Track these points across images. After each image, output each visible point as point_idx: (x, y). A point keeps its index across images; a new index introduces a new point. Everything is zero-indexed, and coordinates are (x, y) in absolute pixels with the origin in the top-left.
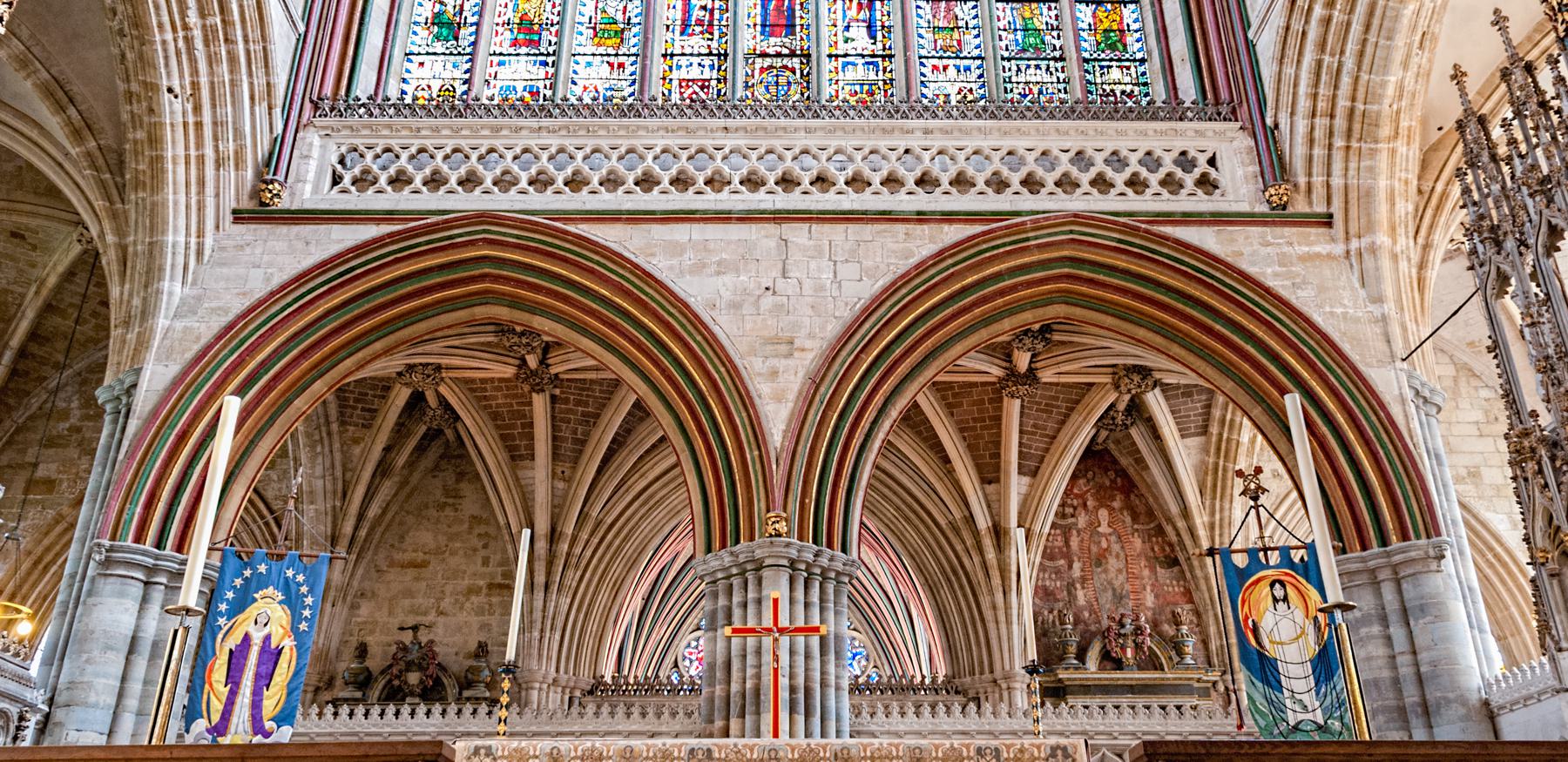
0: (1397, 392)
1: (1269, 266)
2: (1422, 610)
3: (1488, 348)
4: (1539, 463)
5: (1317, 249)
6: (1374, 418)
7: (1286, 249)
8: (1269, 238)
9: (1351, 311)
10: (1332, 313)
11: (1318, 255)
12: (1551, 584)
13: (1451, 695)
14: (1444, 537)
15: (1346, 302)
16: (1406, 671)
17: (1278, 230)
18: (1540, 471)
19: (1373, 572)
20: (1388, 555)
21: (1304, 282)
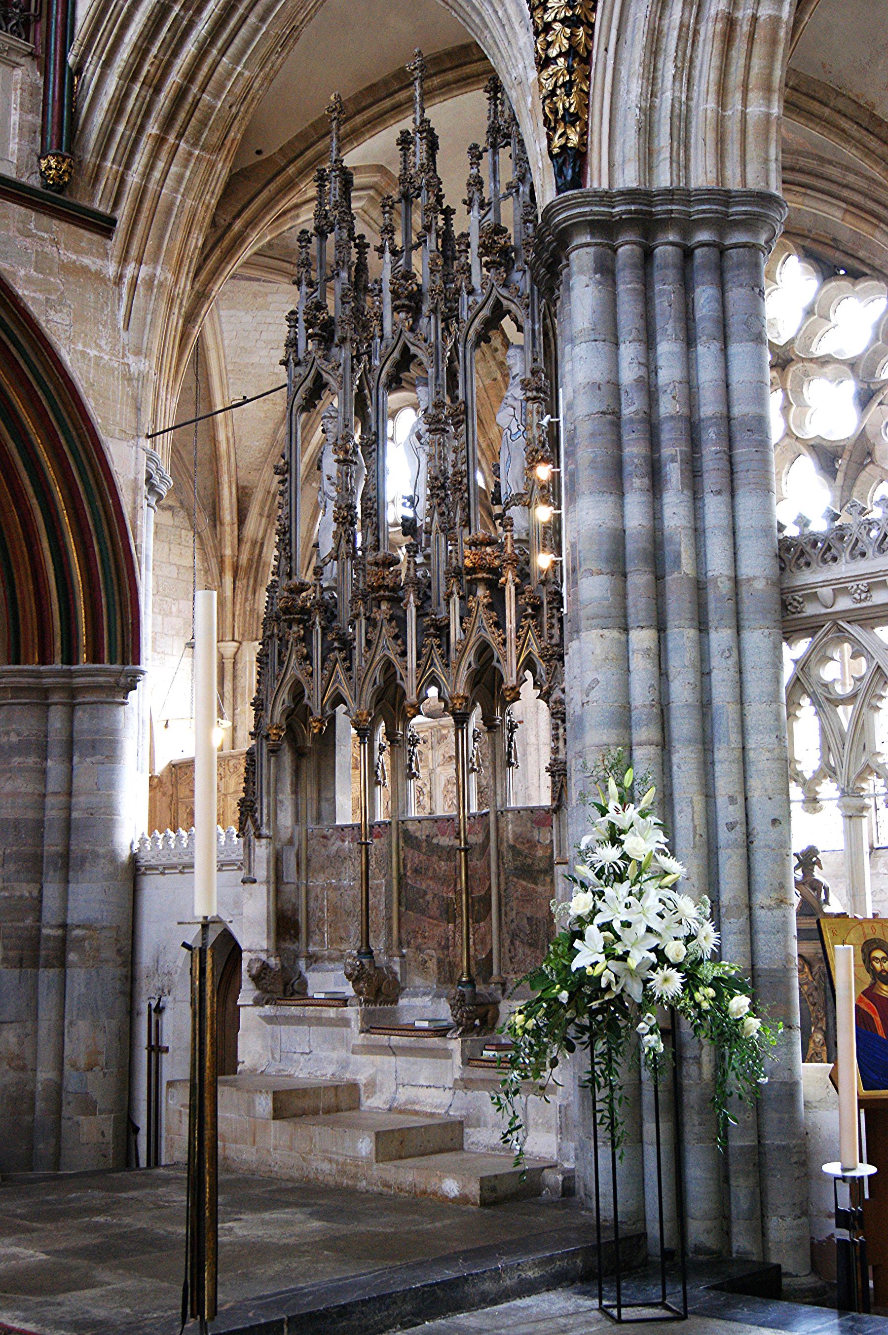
0: (132, 477)
1: (23, 266)
2: (93, 747)
3: (276, 467)
4: (309, 631)
5: (86, 261)
6: (99, 503)
7: (49, 249)
8: (32, 226)
9: (107, 357)
10: (83, 354)
11: (85, 270)
12: (269, 761)
13: (102, 851)
14: (142, 667)
15: (103, 343)
16: (53, 813)
17: (45, 220)
18: (306, 639)
19: (45, 692)
20: (70, 674)
21: (61, 302)
